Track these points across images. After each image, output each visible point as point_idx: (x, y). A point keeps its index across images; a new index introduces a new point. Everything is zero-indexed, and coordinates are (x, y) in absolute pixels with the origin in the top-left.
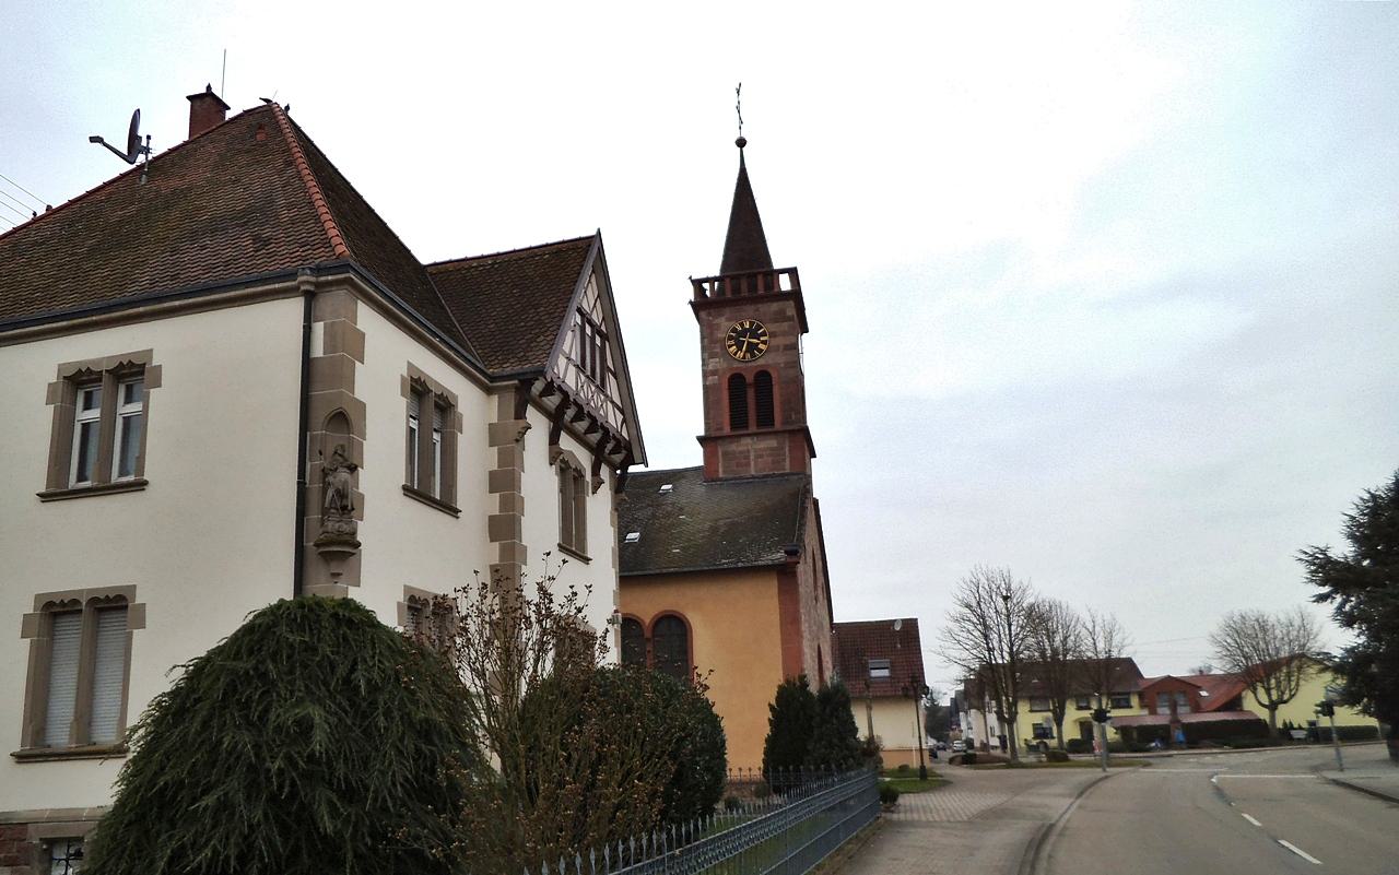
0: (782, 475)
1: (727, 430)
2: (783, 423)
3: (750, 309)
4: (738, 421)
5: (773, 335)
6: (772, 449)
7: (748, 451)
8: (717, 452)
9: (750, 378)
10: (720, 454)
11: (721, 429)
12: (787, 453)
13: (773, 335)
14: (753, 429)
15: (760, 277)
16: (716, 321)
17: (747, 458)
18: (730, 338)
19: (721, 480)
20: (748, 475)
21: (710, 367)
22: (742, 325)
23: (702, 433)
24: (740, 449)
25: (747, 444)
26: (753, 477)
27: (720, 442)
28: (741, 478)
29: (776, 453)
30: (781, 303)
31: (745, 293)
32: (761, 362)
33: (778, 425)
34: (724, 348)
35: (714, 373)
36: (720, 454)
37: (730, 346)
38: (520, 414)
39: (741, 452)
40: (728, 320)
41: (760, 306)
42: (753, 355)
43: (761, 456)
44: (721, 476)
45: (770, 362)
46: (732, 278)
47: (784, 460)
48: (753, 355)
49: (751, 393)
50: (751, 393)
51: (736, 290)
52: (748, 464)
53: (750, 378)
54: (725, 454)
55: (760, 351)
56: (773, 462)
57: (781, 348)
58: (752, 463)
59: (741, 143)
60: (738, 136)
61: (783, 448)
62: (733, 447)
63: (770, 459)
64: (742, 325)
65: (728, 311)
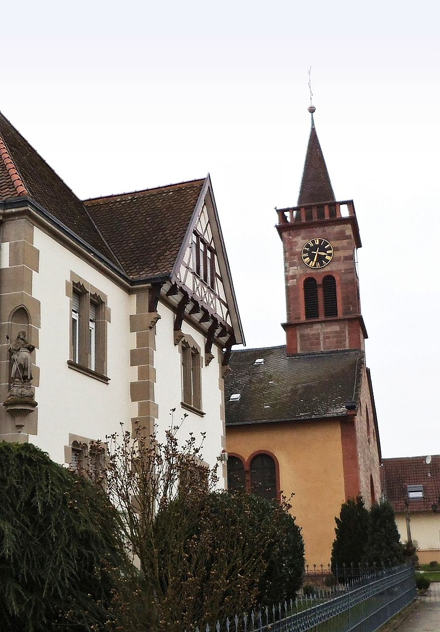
0: (345, 351)
1: (303, 319)
2: (345, 313)
3: (319, 231)
4: (312, 311)
5: (336, 249)
6: (336, 332)
7: (319, 334)
10: (298, 336)
12: (347, 336)
13: (336, 249)
14: (322, 317)
17: (318, 339)
18: (305, 252)
19: (299, 355)
20: (319, 351)
21: (291, 273)
22: (313, 242)
23: (285, 321)
24: (314, 332)
25: (317, 329)
26: (322, 353)
27: (298, 327)
28: (314, 354)
29: (339, 335)
31: (315, 219)
32: (328, 269)
33: (340, 315)
34: (301, 259)
35: (293, 277)
36: (298, 336)
37: (305, 258)
39: (313, 335)
40: (304, 238)
42: (322, 264)
43: (328, 338)
44: (299, 351)
45: (334, 269)
46: (306, 208)
47: (345, 340)
48: (322, 264)
49: (320, 293)
50: (320, 293)
51: (309, 217)
52: (319, 344)
53: (319, 281)
54: (302, 336)
57: (342, 258)
58: (322, 342)
61: (344, 332)
62: (308, 331)
63: (335, 339)
64: (313, 242)
65: (303, 233)
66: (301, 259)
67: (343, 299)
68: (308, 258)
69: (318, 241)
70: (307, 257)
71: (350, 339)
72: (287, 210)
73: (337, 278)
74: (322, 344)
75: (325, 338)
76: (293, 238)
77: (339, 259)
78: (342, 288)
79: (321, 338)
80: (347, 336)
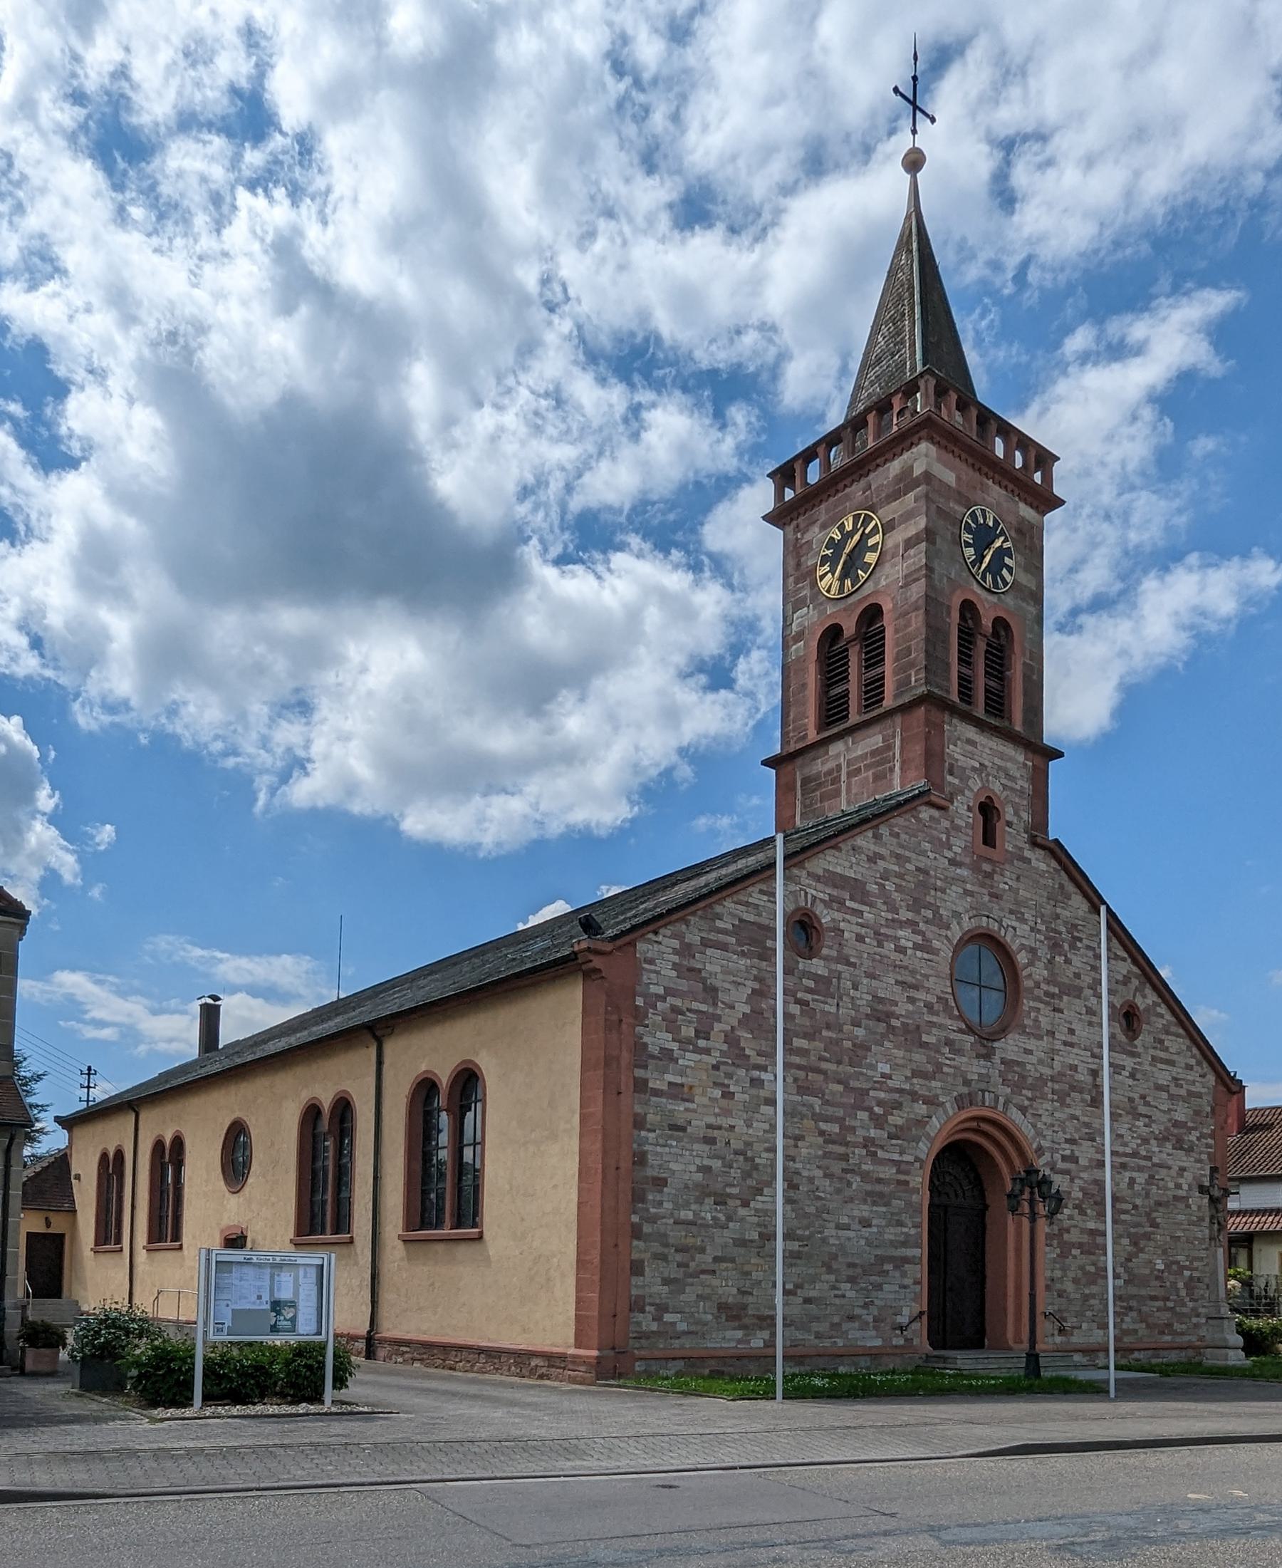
7: (839, 767)
11: (805, 736)
13: (888, 527)
17: (836, 780)
24: (831, 765)
29: (881, 756)
47: (892, 770)
52: (837, 793)
56: (877, 778)
61: (889, 747)
63: (870, 773)
71: (903, 763)
73: (887, 606)
75: (849, 775)
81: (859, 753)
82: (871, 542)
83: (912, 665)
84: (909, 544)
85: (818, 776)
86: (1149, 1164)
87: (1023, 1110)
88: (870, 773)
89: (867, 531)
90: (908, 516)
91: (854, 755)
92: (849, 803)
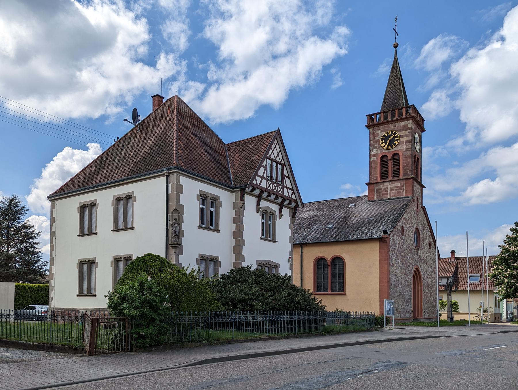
0: (403, 198)
1: (379, 180)
2: (403, 176)
3: (391, 126)
4: (384, 176)
5: (401, 137)
6: (398, 187)
7: (387, 188)
8: (374, 189)
9: (390, 157)
10: (375, 190)
11: (376, 179)
12: (404, 188)
13: (401, 137)
14: (390, 178)
15: (397, 111)
16: (377, 132)
17: (387, 191)
18: (382, 140)
19: (375, 201)
21: (373, 153)
22: (388, 133)
23: (368, 182)
24: (385, 187)
25: (387, 185)
27: (375, 185)
28: (384, 200)
29: (400, 188)
30: (406, 122)
31: (389, 119)
32: (395, 149)
33: (401, 177)
34: (379, 144)
35: (374, 155)
36: (375, 190)
37: (382, 143)
38: (242, 198)
40: (382, 131)
41: (396, 124)
42: (392, 147)
44: (375, 199)
46: (384, 112)
47: (403, 192)
48: (392, 147)
49: (390, 164)
50: (390, 164)
51: (386, 118)
52: (387, 194)
54: (377, 190)
55: (395, 144)
57: (405, 142)
58: (389, 193)
59: (396, 46)
60: (394, 43)
61: (402, 186)
62: (381, 187)
64: (388, 133)
65: (382, 127)
66: (379, 144)
67: (404, 167)
68: (384, 143)
69: (390, 132)
70: (383, 143)
71: (406, 191)
72: (373, 115)
73: (401, 154)
74: (389, 194)
75: (390, 190)
76: (376, 131)
77: (403, 143)
78: (403, 161)
79: (389, 191)
80: (404, 188)
81: (393, 186)
82: (396, 139)
83: (408, 169)
84: (407, 142)
85: (381, 189)
86: (431, 277)
87: (420, 266)
88: (397, 191)
89: (395, 136)
90: (406, 136)
91: (392, 186)
92: (390, 197)
